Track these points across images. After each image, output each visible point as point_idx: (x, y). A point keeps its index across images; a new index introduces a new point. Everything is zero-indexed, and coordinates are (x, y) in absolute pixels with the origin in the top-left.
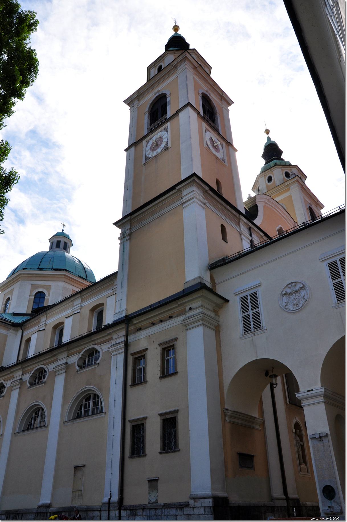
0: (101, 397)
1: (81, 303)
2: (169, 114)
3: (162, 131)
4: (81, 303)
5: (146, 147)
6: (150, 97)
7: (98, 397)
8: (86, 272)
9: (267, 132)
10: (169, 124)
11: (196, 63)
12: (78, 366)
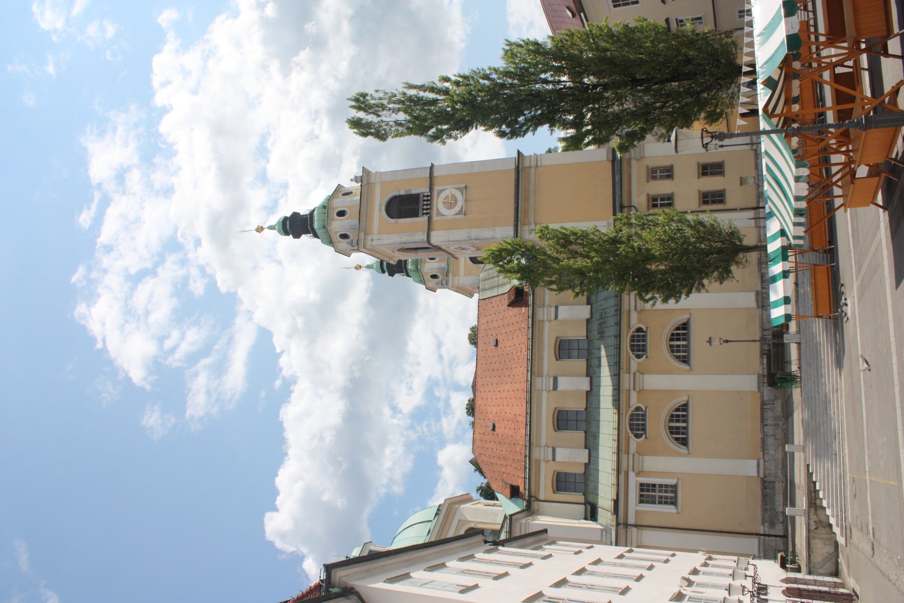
3: (438, 196)
5: (443, 215)
10: (436, 188)
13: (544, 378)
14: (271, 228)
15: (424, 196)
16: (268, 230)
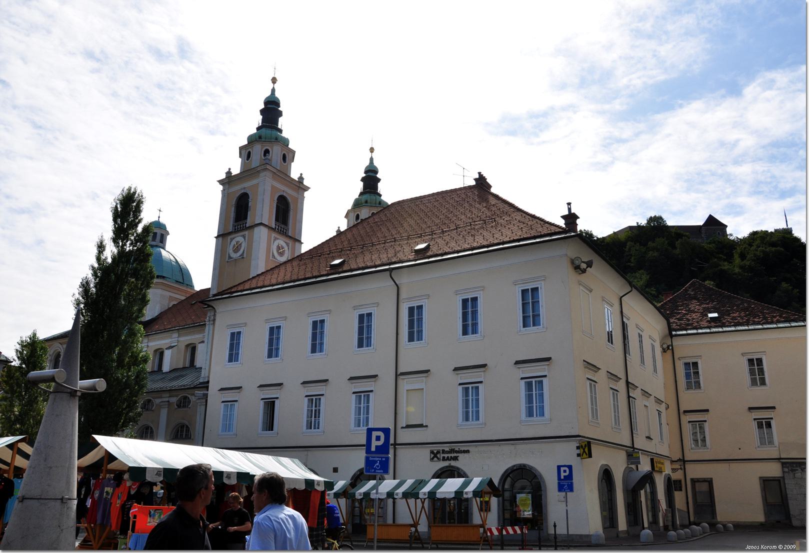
0: (190, 429)
1: (178, 337)
2: (249, 222)
3: (241, 236)
4: (178, 337)
6: (238, 189)
7: (189, 428)
8: (182, 274)
9: (372, 150)
10: (246, 233)
11: (275, 170)
12: (177, 405)
13: (176, 339)
14: (273, 90)
15: (246, 223)
16: (272, 88)
